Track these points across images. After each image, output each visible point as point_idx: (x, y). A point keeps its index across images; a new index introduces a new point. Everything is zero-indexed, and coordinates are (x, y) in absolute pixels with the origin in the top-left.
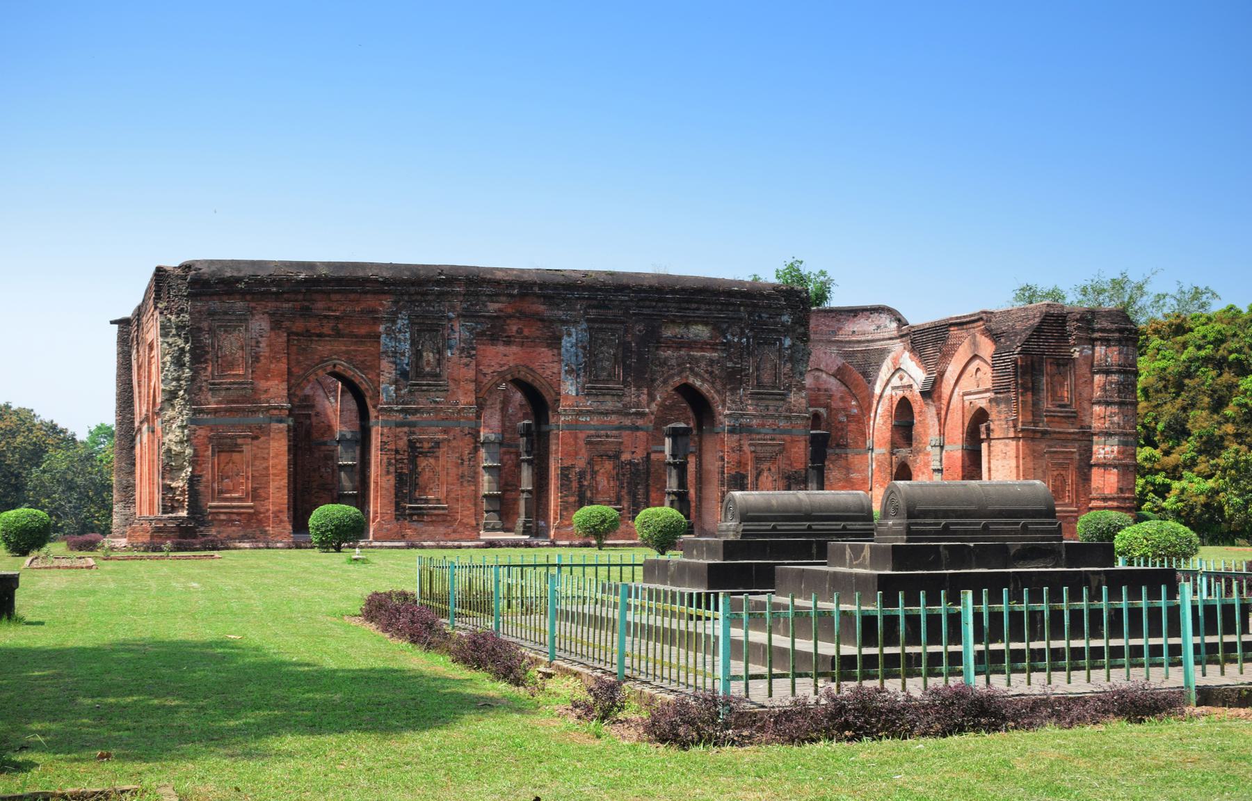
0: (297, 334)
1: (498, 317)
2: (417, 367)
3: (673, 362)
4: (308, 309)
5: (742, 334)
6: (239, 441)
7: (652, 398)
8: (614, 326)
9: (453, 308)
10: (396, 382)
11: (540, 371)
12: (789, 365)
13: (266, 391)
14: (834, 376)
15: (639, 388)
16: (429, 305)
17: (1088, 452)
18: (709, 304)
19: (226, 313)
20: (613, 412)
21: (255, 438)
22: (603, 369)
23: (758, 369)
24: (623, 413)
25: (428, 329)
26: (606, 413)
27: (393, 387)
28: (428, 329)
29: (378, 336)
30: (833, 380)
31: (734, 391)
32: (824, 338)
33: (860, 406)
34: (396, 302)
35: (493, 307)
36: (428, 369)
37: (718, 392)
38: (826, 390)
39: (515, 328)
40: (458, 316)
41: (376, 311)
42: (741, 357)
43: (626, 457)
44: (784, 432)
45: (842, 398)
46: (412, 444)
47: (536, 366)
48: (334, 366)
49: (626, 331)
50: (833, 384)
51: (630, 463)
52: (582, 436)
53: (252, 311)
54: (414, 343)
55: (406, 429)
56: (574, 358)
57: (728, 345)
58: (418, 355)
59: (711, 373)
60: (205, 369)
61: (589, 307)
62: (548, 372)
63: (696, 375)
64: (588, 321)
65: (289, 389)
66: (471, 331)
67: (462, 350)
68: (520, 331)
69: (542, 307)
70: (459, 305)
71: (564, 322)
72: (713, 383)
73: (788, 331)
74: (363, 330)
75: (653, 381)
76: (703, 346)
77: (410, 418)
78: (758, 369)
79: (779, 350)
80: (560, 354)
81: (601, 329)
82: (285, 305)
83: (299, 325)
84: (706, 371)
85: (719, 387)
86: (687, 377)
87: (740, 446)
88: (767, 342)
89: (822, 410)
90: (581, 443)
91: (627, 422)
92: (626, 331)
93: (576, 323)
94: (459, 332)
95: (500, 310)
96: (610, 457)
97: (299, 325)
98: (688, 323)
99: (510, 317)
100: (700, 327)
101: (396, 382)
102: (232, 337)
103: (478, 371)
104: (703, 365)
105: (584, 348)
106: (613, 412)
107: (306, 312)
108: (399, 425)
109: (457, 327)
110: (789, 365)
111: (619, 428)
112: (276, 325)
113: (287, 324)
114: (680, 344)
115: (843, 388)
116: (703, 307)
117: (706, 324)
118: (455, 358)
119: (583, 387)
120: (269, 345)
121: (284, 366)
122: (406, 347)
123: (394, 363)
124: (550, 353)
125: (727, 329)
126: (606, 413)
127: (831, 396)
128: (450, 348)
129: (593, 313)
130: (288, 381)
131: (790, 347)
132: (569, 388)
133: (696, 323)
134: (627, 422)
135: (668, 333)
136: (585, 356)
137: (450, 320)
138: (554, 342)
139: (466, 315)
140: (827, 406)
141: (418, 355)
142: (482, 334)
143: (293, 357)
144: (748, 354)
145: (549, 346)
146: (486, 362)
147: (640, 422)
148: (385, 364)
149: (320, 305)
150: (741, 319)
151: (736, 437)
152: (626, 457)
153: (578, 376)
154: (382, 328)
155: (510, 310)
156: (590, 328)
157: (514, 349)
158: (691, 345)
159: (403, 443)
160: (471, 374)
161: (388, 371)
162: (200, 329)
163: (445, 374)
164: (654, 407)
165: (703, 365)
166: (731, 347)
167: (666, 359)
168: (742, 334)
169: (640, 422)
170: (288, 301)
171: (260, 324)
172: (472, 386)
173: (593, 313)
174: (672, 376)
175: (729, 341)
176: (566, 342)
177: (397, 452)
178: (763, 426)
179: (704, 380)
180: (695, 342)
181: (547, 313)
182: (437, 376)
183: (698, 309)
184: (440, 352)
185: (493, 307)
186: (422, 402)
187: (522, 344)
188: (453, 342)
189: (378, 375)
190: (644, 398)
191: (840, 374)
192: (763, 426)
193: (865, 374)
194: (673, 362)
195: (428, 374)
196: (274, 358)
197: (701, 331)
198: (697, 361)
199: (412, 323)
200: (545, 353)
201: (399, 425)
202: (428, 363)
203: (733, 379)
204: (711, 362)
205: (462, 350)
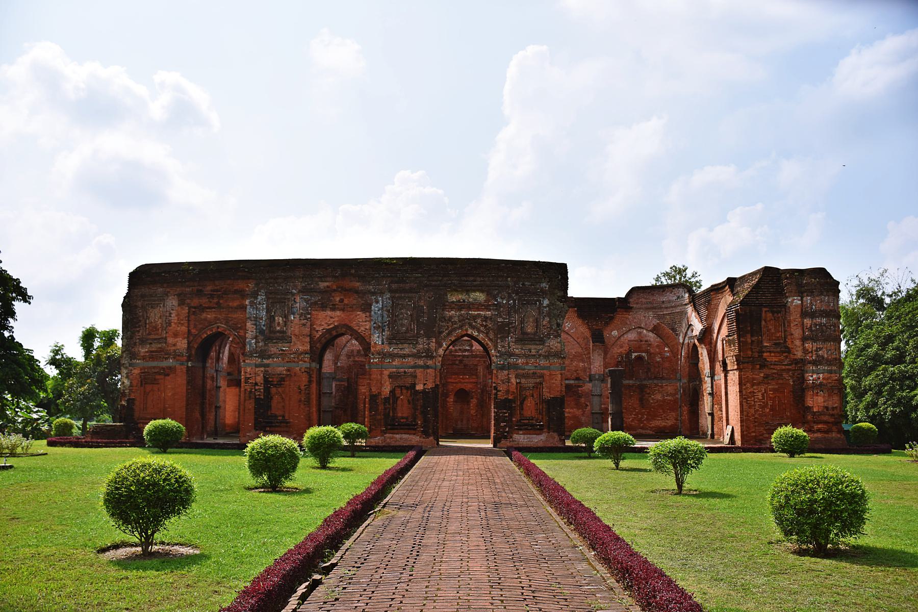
0: (195, 308)
1: (326, 292)
2: (271, 327)
3: (456, 319)
4: (201, 290)
5: (510, 298)
6: (158, 377)
7: (440, 345)
8: (410, 295)
9: (295, 287)
10: (256, 337)
11: (356, 328)
12: (547, 319)
13: (174, 345)
14: (652, 331)
15: (429, 338)
16: (279, 285)
17: (803, 379)
18: (483, 277)
19: (151, 296)
20: (409, 356)
21: (168, 375)
22: (402, 325)
23: (522, 322)
24: (417, 356)
25: (278, 301)
26: (404, 356)
27: (254, 341)
28: (278, 301)
29: (244, 308)
30: (651, 334)
31: (503, 339)
32: (644, 306)
33: (671, 351)
34: (257, 285)
35: (323, 285)
36: (278, 328)
37: (490, 340)
38: (646, 341)
39: (338, 299)
40: (300, 291)
41: (243, 291)
42: (509, 314)
43: (419, 387)
44: (544, 368)
45: (657, 346)
46: (266, 380)
47: (353, 325)
48: (218, 327)
49: (420, 298)
50: (651, 336)
51: (424, 392)
52: (386, 373)
53: (167, 294)
54: (268, 311)
55: (262, 369)
56: (380, 319)
57: (499, 305)
58: (271, 319)
59: (485, 326)
60: (139, 331)
61: (392, 282)
62: (362, 329)
63: (473, 328)
64: (391, 291)
65: (189, 343)
66: (307, 301)
67: (301, 315)
68: (341, 301)
69: (358, 284)
70: (300, 285)
71: (374, 294)
72: (487, 333)
73: (544, 293)
74: (236, 304)
75: (441, 333)
76: (478, 306)
77: (265, 361)
78: (522, 322)
79: (539, 308)
80: (370, 316)
81: (400, 298)
82: (188, 289)
83: (195, 302)
84: (482, 325)
85: (491, 336)
86: (467, 330)
87: (509, 379)
88: (529, 303)
89: (644, 354)
90: (386, 378)
91: (421, 362)
92: (420, 298)
93: (382, 293)
94: (299, 303)
95: (328, 287)
96: (407, 388)
97: (195, 302)
98: (468, 292)
99: (335, 290)
100: (477, 294)
101: (256, 337)
102: (156, 311)
103: (312, 328)
104: (479, 321)
105: (388, 311)
106: (409, 356)
107: (200, 293)
108: (257, 366)
109: (298, 299)
110: (547, 319)
111: (415, 367)
112: (181, 303)
113: (188, 301)
114: (460, 306)
115: (659, 339)
116: (478, 279)
117: (482, 291)
118: (297, 320)
119: (387, 339)
120: (178, 315)
121: (184, 329)
122: (264, 314)
123: (255, 324)
124: (364, 315)
125: (498, 294)
126: (404, 356)
127: (650, 345)
128: (294, 314)
129: (394, 286)
130: (188, 337)
131: (548, 306)
132: (376, 339)
133: (475, 291)
134: (421, 363)
135: (453, 298)
136: (388, 316)
137: (293, 294)
138: (367, 308)
139: (303, 291)
140: (647, 351)
141: (271, 319)
142: (315, 303)
143: (192, 323)
144: (515, 312)
145: (364, 311)
146: (318, 322)
147: (430, 362)
148: (249, 325)
149: (209, 288)
150: (509, 287)
151: (506, 372)
152: (419, 387)
153: (383, 331)
154: (247, 302)
155: (335, 287)
156: (392, 298)
157: (338, 313)
158: (470, 306)
159: (260, 379)
160: (307, 330)
161: (251, 330)
162: (136, 307)
163: (289, 333)
164: (441, 351)
165: (479, 321)
166: (501, 307)
167: (451, 317)
168: (510, 298)
169: (430, 362)
170: (188, 286)
171: (172, 302)
172: (308, 339)
173: (394, 286)
174: (455, 329)
175: (499, 303)
176: (375, 308)
177: (256, 384)
178: (527, 363)
179: (479, 331)
180: (473, 304)
181: (361, 288)
182: (284, 332)
183: (475, 281)
184: (286, 317)
185: (323, 285)
186: (273, 349)
187: (343, 310)
188: (295, 310)
189: (246, 333)
190: (433, 345)
191: (655, 330)
192: (527, 363)
193: (674, 330)
194: (456, 319)
195: (279, 332)
196: (180, 323)
197: (480, 296)
198: (475, 318)
199: (268, 298)
200: (361, 315)
201: (257, 366)
202: (279, 323)
203: (502, 331)
204: (486, 318)
205: (301, 315)
